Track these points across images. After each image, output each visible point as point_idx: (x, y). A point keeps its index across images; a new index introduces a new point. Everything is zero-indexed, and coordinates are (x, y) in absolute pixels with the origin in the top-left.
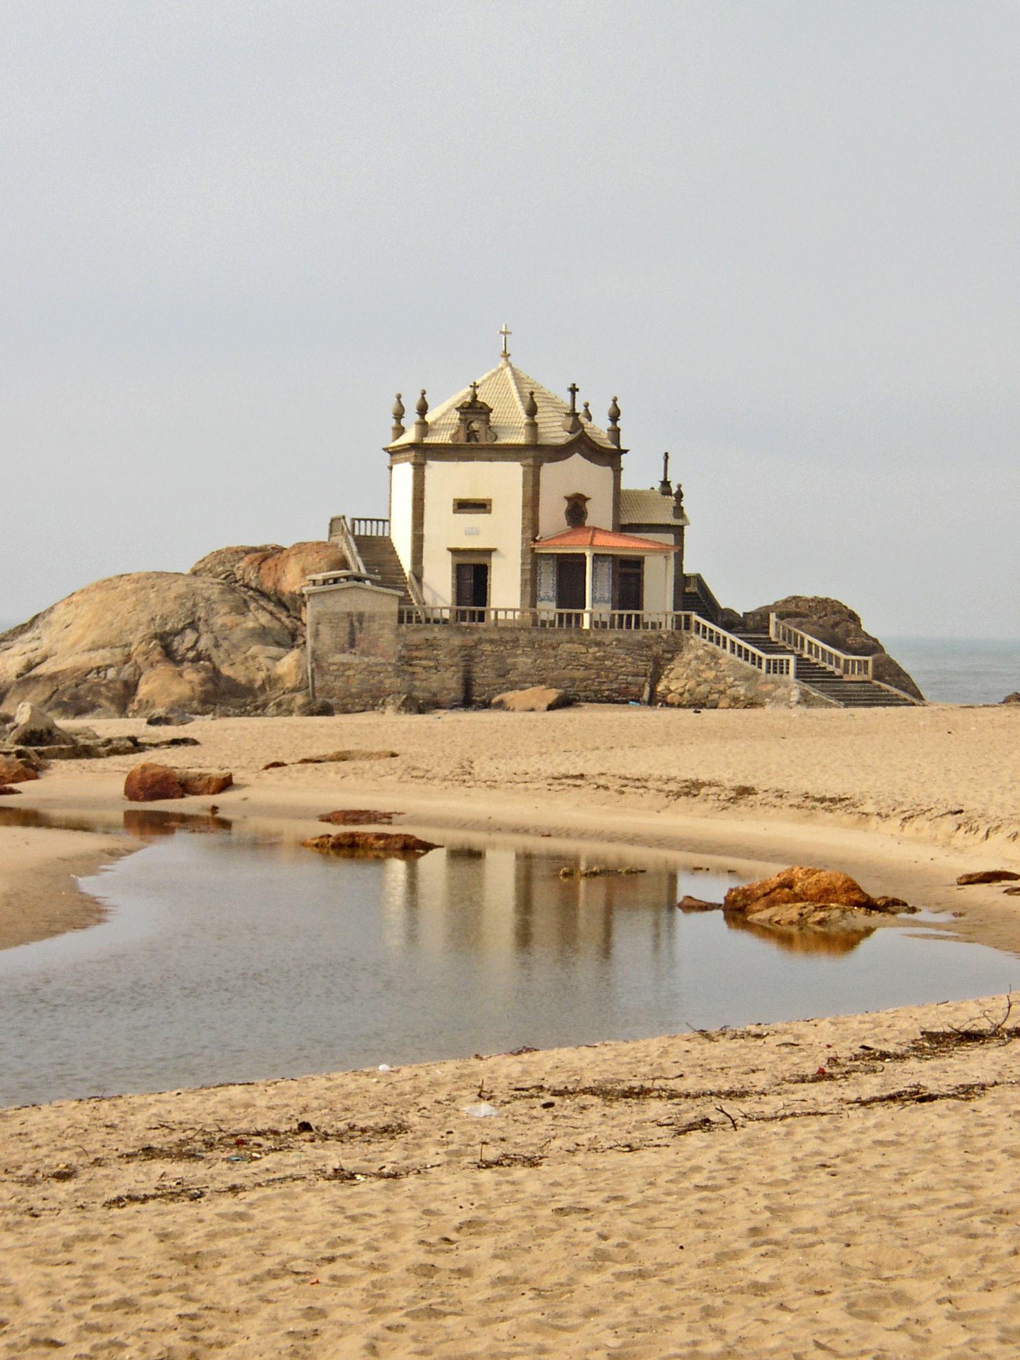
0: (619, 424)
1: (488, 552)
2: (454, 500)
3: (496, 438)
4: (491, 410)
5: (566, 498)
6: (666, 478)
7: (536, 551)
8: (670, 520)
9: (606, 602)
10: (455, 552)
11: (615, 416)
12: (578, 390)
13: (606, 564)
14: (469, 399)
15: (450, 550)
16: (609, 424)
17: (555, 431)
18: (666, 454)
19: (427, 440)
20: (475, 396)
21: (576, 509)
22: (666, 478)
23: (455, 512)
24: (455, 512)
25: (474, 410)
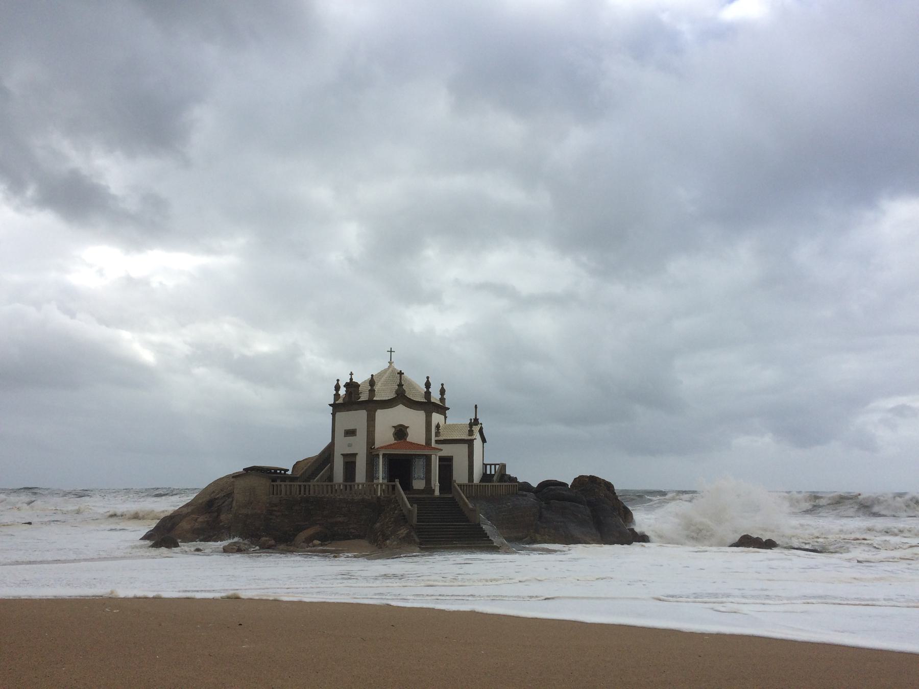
0: (430, 390)
1: (355, 455)
2: (345, 430)
3: (360, 397)
4: (359, 385)
5: (393, 426)
6: (476, 417)
7: (373, 454)
9: (422, 479)
10: (344, 455)
11: (428, 385)
12: (403, 373)
13: (422, 459)
14: (349, 381)
15: (342, 454)
16: (425, 390)
17: (384, 393)
18: (476, 405)
19: (337, 402)
20: (351, 379)
21: (401, 432)
22: (476, 417)
23: (345, 436)
24: (345, 436)
25: (352, 386)
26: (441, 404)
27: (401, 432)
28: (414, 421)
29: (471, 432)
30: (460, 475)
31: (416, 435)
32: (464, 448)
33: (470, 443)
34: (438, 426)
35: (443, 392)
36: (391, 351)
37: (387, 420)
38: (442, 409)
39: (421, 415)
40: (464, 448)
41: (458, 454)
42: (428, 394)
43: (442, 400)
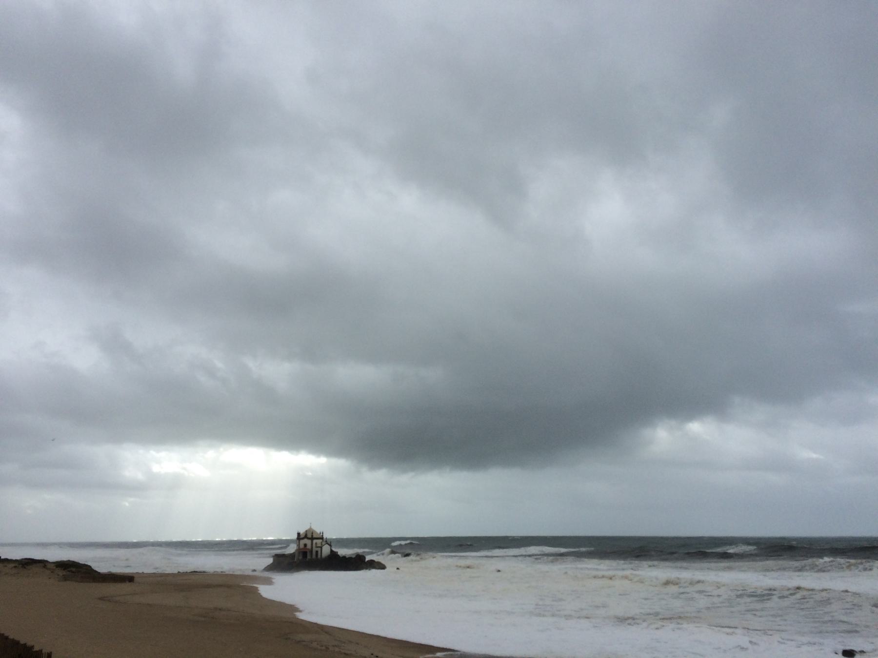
8: (320, 545)
21: (305, 545)
26: (321, 537)
27: (305, 545)
28: (308, 542)
29: (322, 544)
30: (319, 556)
31: (309, 546)
32: (320, 549)
33: (321, 547)
34: (316, 543)
35: (323, 533)
36: (311, 524)
37: (303, 542)
38: (322, 538)
39: (310, 541)
40: (320, 549)
41: (319, 549)
42: (312, 536)
43: (322, 536)
